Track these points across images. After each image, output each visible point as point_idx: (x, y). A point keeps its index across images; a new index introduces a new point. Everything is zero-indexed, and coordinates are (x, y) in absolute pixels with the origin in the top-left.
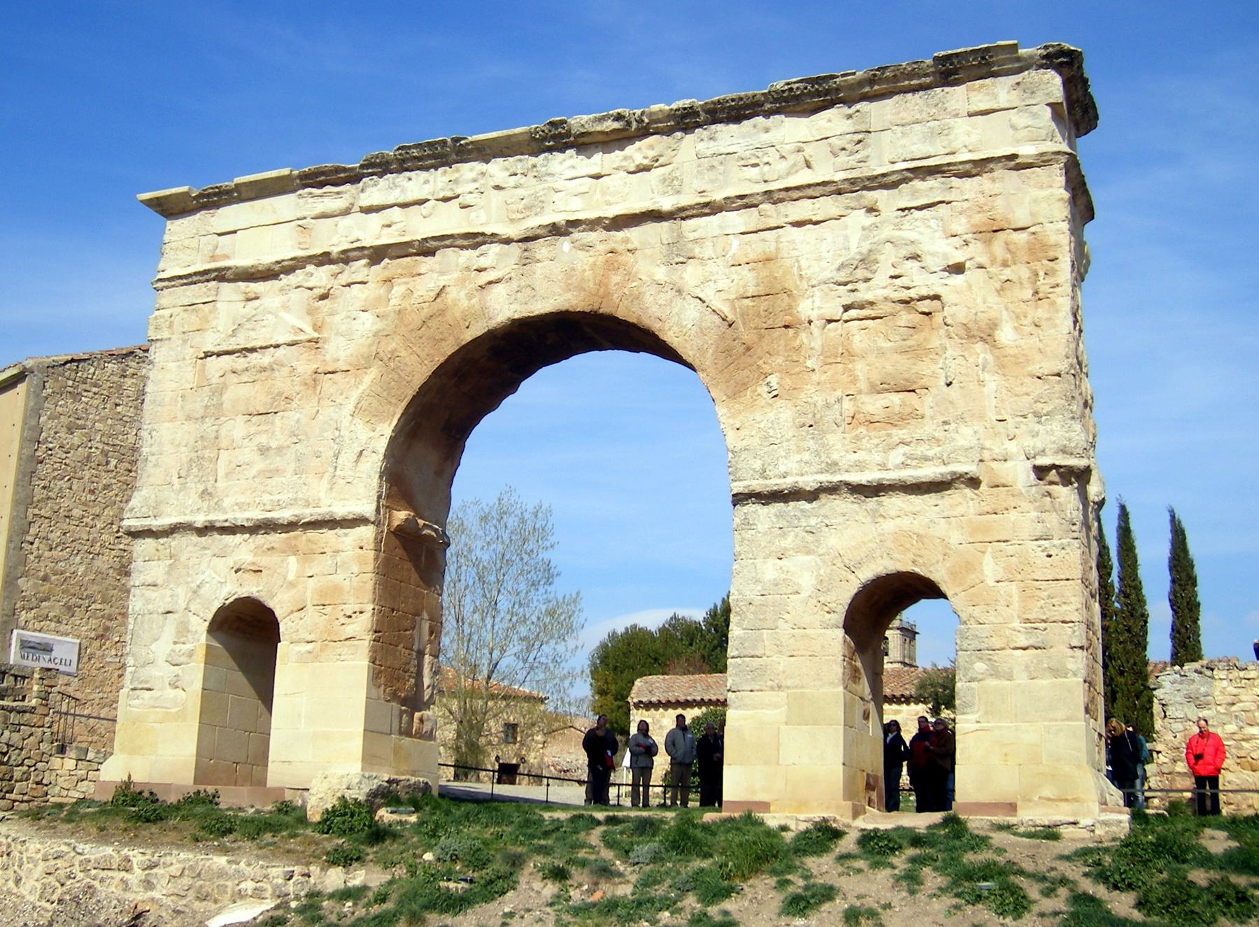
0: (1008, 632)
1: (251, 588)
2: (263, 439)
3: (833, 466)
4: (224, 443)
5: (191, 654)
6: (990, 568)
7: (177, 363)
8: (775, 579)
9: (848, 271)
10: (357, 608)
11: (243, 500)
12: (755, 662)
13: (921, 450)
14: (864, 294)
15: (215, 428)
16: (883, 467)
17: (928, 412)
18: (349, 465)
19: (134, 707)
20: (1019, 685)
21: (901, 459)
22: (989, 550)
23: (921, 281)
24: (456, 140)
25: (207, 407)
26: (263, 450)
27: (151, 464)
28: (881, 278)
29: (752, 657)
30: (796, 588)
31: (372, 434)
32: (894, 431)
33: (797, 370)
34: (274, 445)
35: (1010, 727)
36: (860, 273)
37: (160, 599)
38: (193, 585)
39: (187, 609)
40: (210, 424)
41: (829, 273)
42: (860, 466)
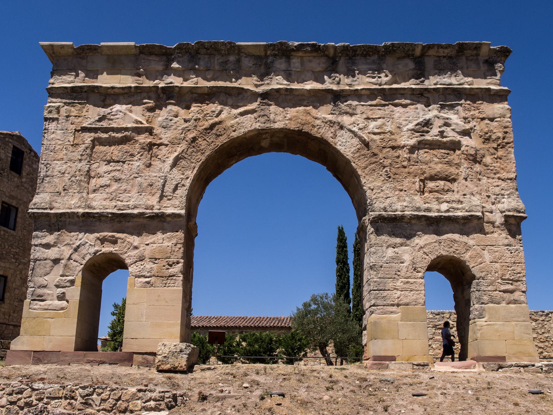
0: (497, 284)
1: (108, 248)
2: (117, 174)
3: (418, 209)
4: (93, 174)
5: (72, 282)
6: (487, 256)
7: (63, 131)
8: (392, 256)
9: (420, 126)
10: (175, 260)
11: (105, 204)
12: (385, 293)
13: (454, 205)
14: (428, 137)
15: (88, 166)
16: (439, 211)
17: (456, 190)
18: (171, 190)
19: (35, 309)
20: (503, 306)
21: (446, 208)
22: (487, 249)
23: (451, 135)
24: (230, 43)
25: (82, 155)
26: (118, 180)
27: (46, 182)
28: (435, 131)
29: (384, 290)
30: (402, 261)
31: (182, 176)
32: (442, 196)
33: (398, 166)
34: (123, 177)
35: (500, 324)
36: (425, 129)
37: (53, 253)
38: (74, 246)
39: (70, 259)
40: (84, 164)
41: (411, 126)
42: (428, 210)
